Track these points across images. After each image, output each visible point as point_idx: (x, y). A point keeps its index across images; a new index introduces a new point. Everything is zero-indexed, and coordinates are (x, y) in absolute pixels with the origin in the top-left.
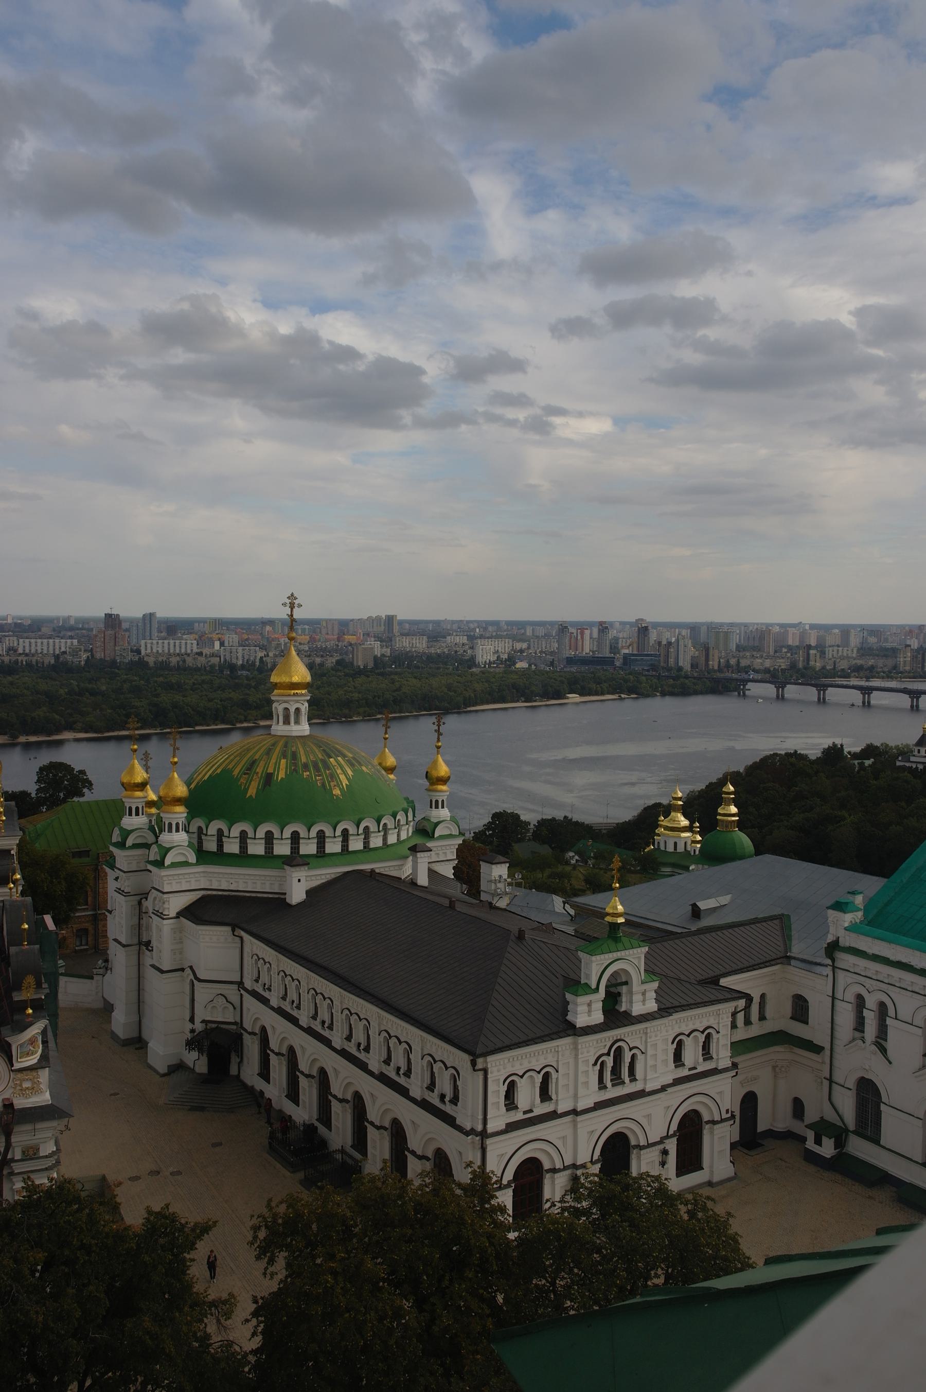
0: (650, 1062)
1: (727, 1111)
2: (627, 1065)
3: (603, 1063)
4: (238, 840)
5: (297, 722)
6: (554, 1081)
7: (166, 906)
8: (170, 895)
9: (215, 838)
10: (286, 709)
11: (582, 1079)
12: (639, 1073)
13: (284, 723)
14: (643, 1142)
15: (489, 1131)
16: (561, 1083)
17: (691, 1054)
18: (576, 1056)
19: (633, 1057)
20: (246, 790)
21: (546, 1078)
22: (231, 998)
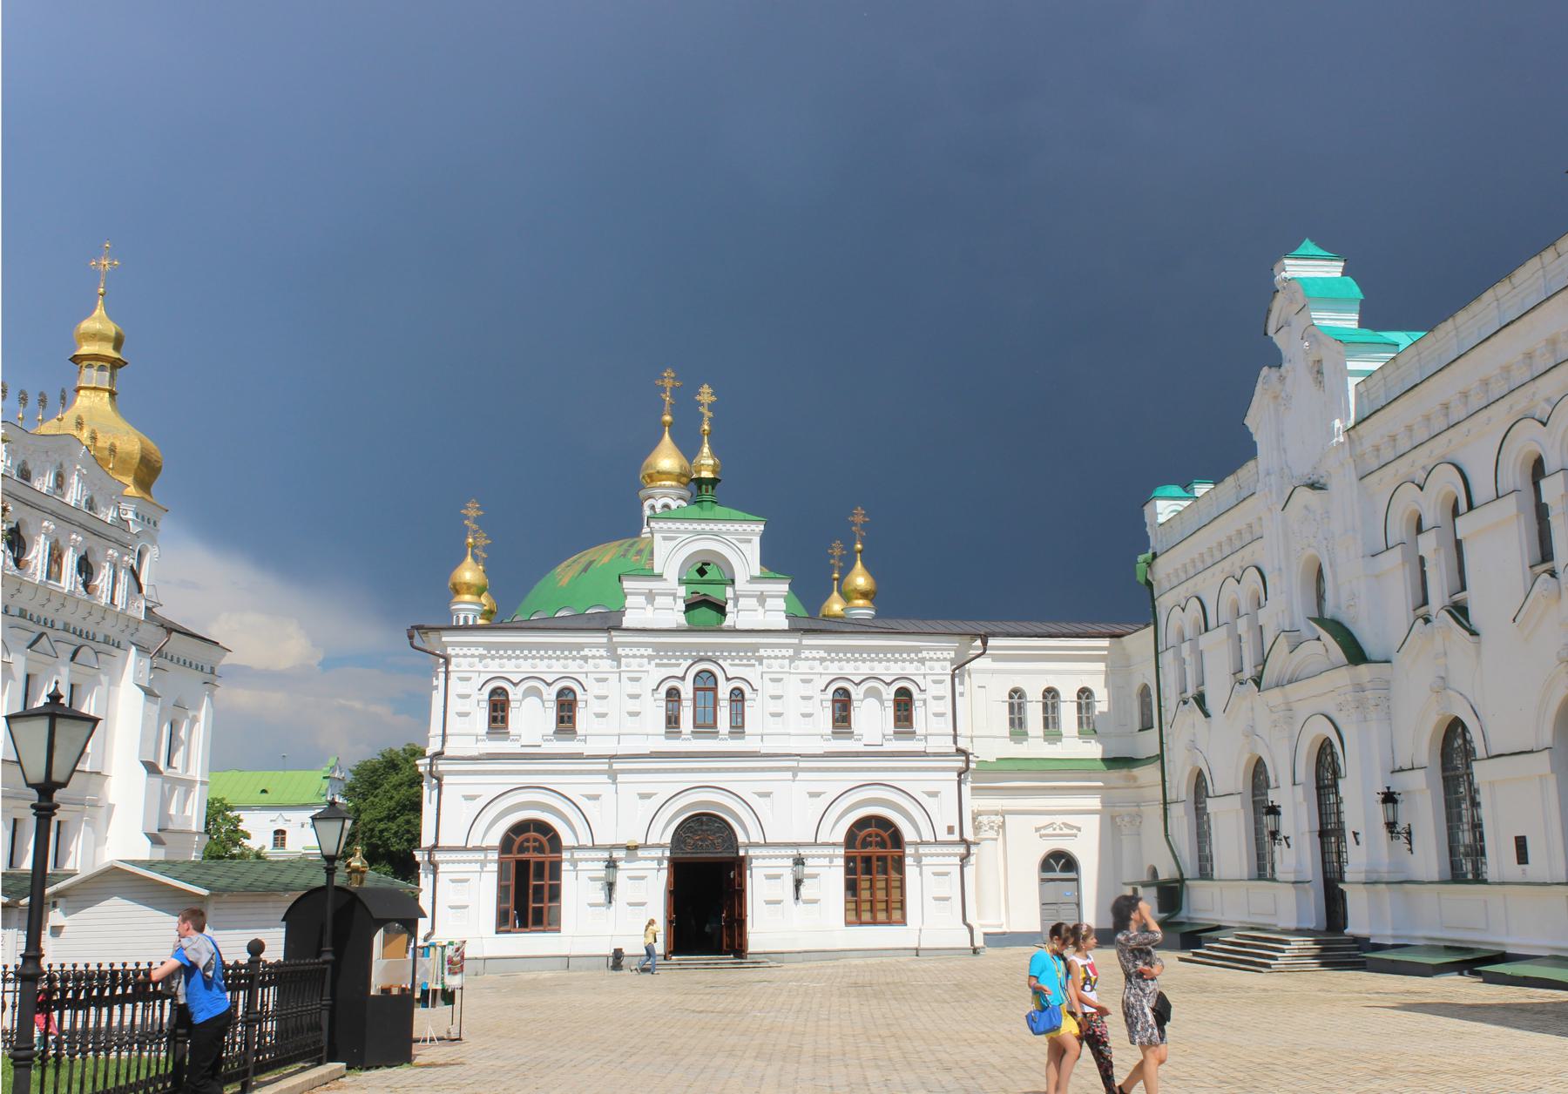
1: (950, 830)
2: (722, 703)
3: (673, 695)
14: (756, 837)
15: (447, 753)
17: (873, 719)
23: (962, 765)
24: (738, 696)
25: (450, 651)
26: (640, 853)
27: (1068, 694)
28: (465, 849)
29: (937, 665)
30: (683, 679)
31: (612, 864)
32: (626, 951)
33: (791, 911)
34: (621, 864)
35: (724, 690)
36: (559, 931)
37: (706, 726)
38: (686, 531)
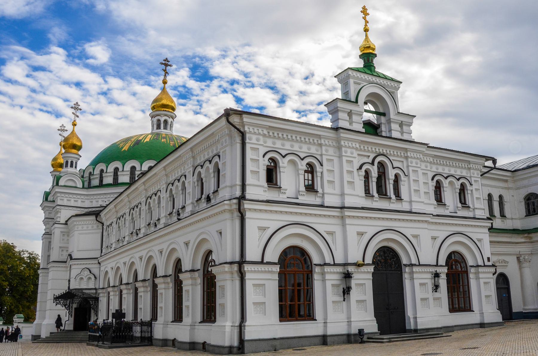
0: (414, 187)
2: (392, 182)
4: (112, 174)
5: (165, 128)
6: (319, 174)
7: (59, 215)
8: (62, 208)
9: (98, 176)
10: (159, 120)
11: (347, 178)
12: (404, 194)
13: (157, 129)
14: (414, 261)
15: (248, 196)
16: (327, 177)
18: (340, 157)
19: (397, 176)
20: (122, 148)
21: (311, 169)
22: (93, 271)
23: (490, 225)
24: (397, 178)
25: (246, 129)
26: (363, 269)
27: (496, 198)
28: (262, 262)
29: (476, 172)
30: (373, 163)
31: (348, 276)
32: (366, 331)
33: (426, 305)
34: (355, 276)
35: (391, 174)
36: (281, 321)
37: (382, 192)
38: (365, 80)
